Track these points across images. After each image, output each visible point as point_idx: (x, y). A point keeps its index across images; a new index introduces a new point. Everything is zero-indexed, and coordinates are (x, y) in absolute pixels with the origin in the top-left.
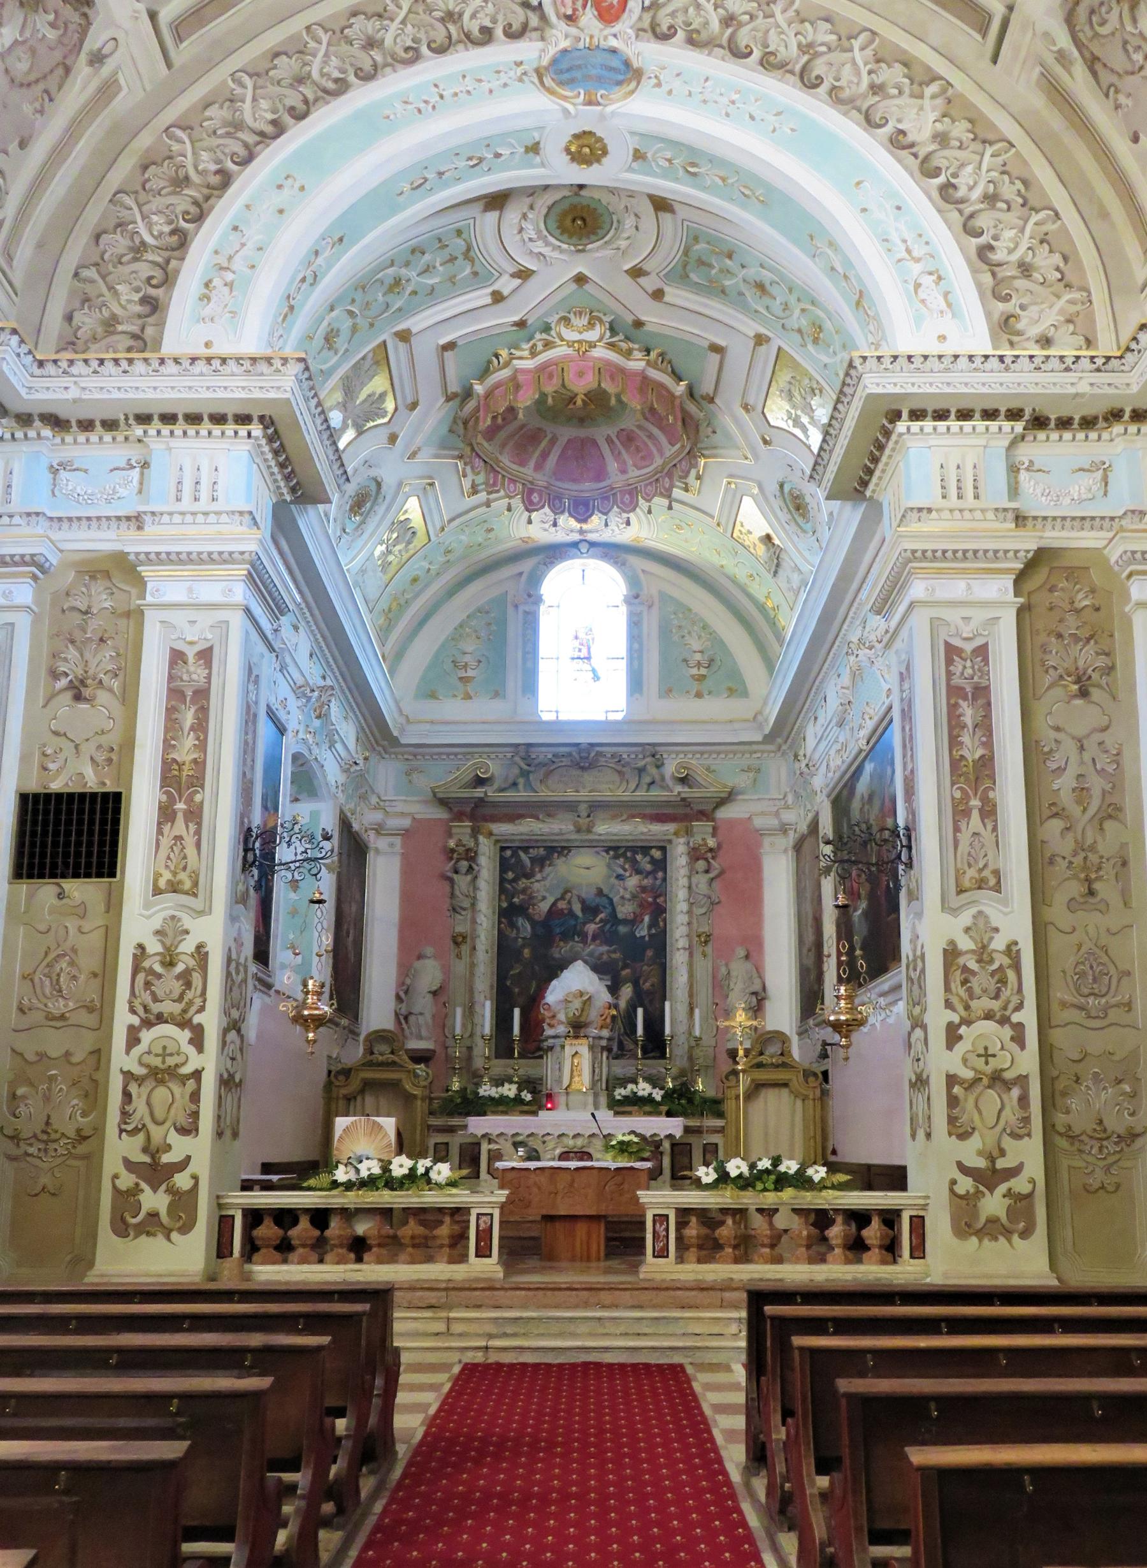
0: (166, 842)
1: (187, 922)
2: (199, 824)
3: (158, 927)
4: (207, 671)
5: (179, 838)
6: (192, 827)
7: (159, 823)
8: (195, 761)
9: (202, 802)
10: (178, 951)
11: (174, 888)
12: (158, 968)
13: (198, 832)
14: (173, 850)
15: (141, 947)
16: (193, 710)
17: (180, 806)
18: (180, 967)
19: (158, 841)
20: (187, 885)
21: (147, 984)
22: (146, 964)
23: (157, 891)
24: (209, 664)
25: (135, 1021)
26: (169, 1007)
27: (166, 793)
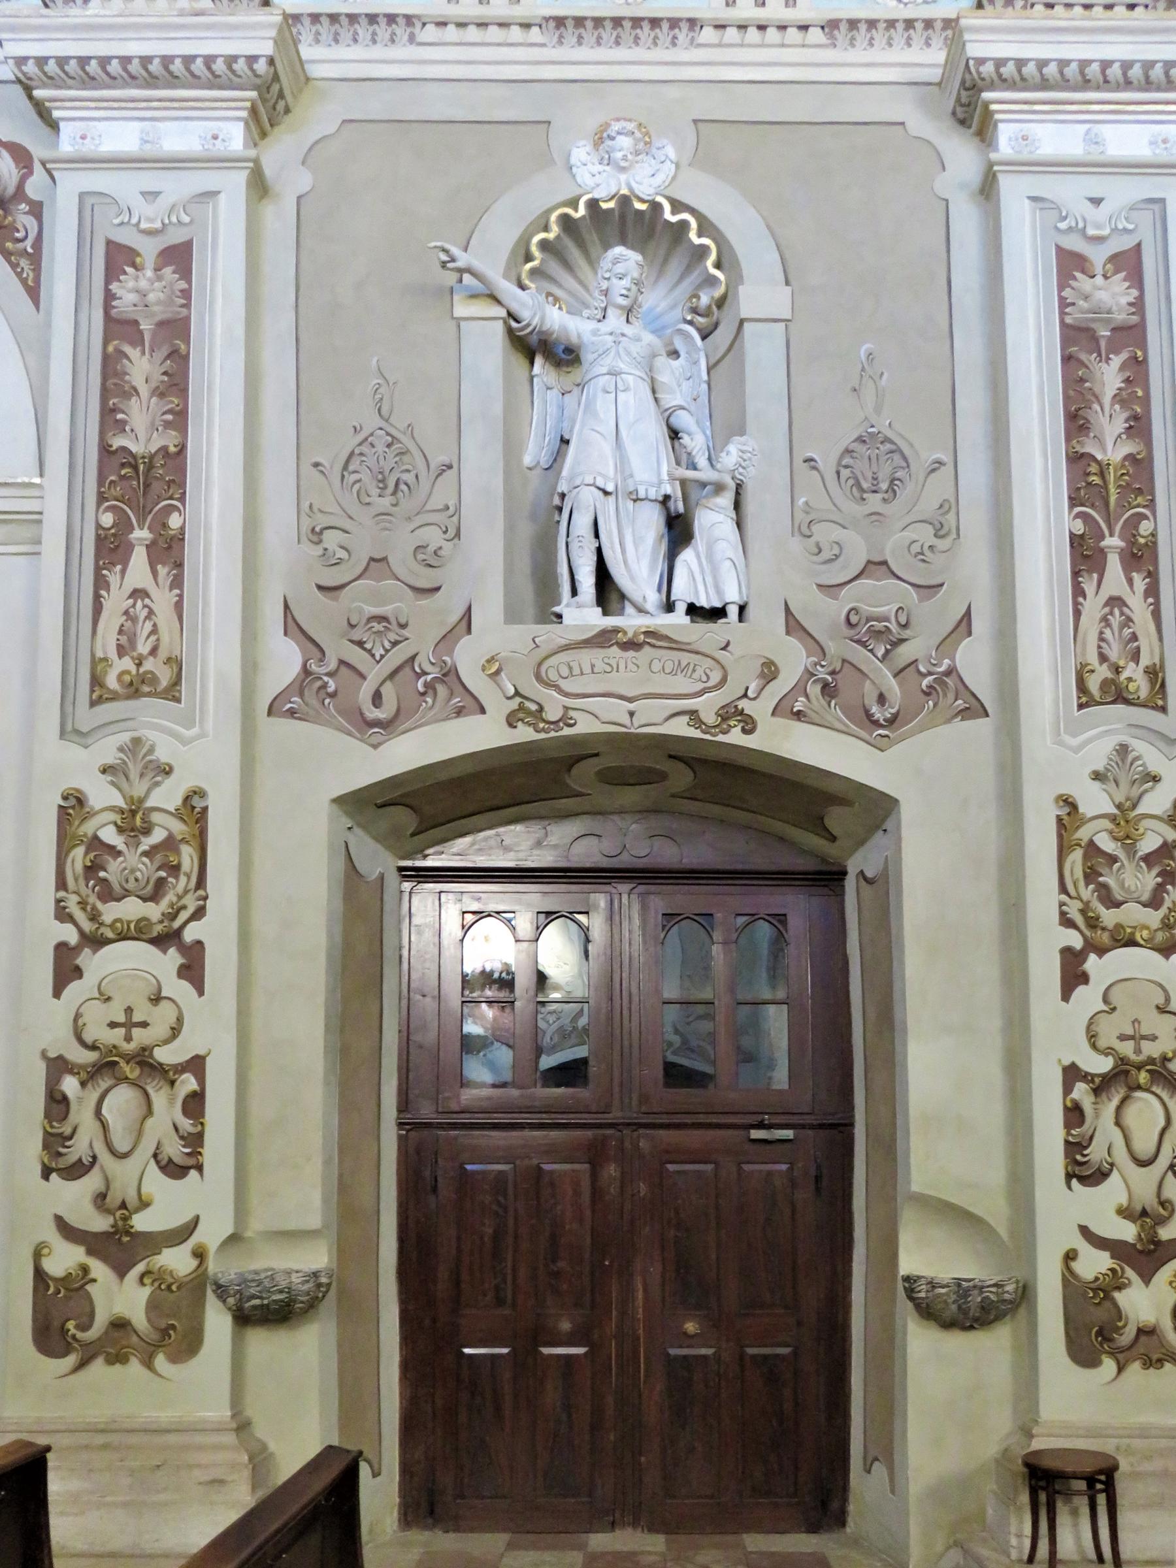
0: (1093, 606)
1: (1151, 756)
2: (1153, 576)
3: (1100, 767)
4: (1135, 292)
5: (1115, 602)
6: (1140, 583)
7: (1076, 574)
8: (1130, 458)
9: (1153, 535)
10: (1140, 810)
11: (1118, 694)
12: (1107, 844)
13: (1153, 591)
14: (1108, 625)
15: (1069, 803)
16: (1117, 361)
17: (1113, 542)
18: (1148, 844)
19: (1076, 604)
20: (1141, 686)
21: (1091, 875)
22: (1084, 834)
23: (1086, 700)
24: (1136, 278)
25: (1075, 940)
26: (1133, 915)
27: (1082, 516)
